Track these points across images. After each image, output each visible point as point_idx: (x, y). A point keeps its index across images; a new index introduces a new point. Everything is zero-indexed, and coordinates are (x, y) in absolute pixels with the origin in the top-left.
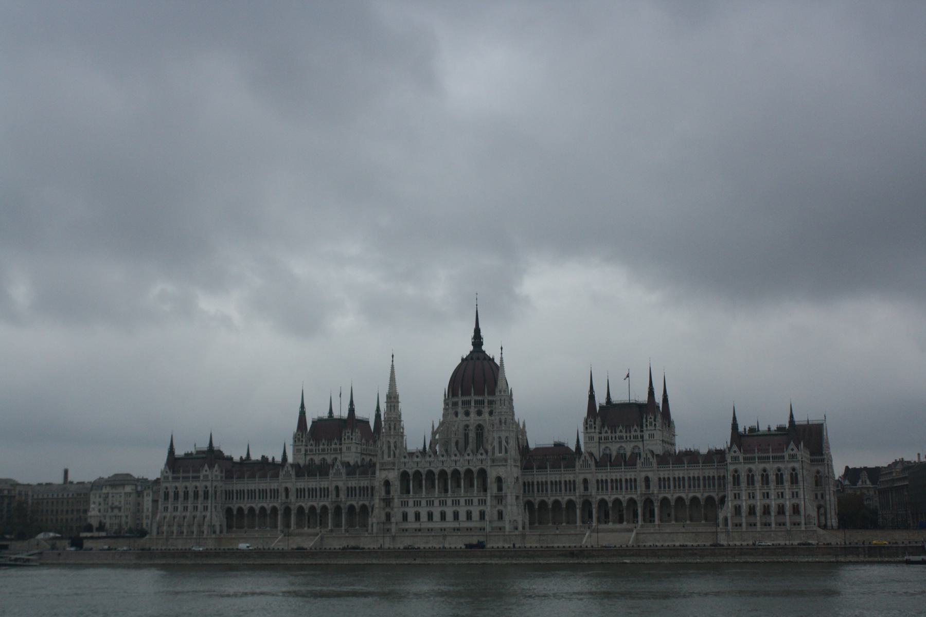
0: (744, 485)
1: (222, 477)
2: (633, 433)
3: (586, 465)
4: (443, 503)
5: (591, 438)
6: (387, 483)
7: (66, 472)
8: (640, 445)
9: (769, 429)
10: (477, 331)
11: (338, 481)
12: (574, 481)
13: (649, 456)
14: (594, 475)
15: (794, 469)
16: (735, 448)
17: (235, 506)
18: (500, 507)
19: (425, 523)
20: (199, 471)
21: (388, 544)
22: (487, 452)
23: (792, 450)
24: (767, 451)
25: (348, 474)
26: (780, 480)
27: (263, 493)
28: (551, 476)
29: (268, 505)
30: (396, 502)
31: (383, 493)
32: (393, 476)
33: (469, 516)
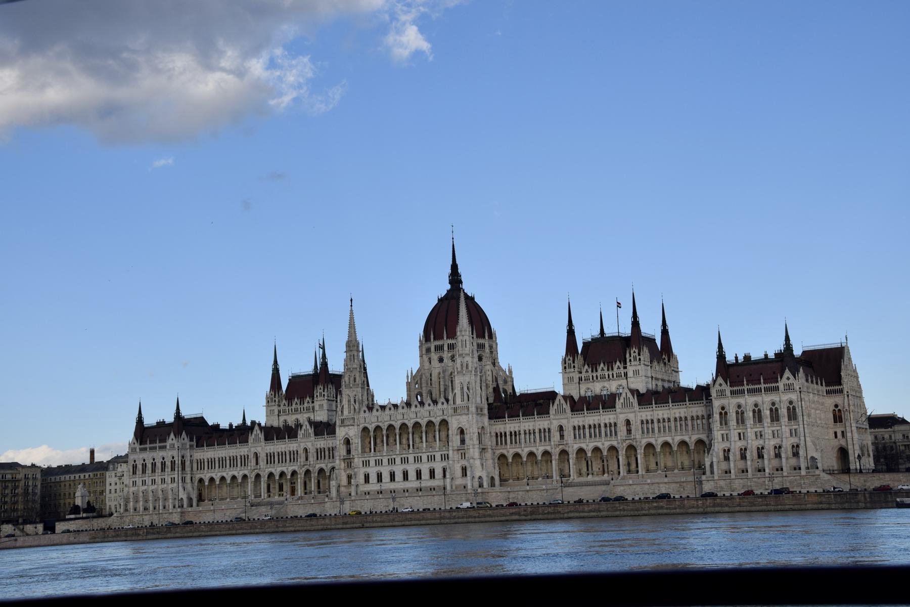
0: (733, 422)
1: (191, 446)
3: (561, 411)
4: (405, 461)
5: (571, 379)
6: (348, 442)
7: (92, 452)
9: (766, 355)
10: (454, 267)
11: (307, 441)
12: (549, 429)
13: (629, 395)
14: (571, 421)
15: (791, 402)
16: (720, 380)
17: (206, 475)
19: (387, 484)
20: (164, 440)
21: (330, 508)
22: (447, 400)
23: (788, 379)
25: (316, 435)
26: (775, 416)
27: (233, 461)
28: (523, 424)
29: (239, 473)
30: (358, 462)
32: (353, 432)
33: (432, 474)
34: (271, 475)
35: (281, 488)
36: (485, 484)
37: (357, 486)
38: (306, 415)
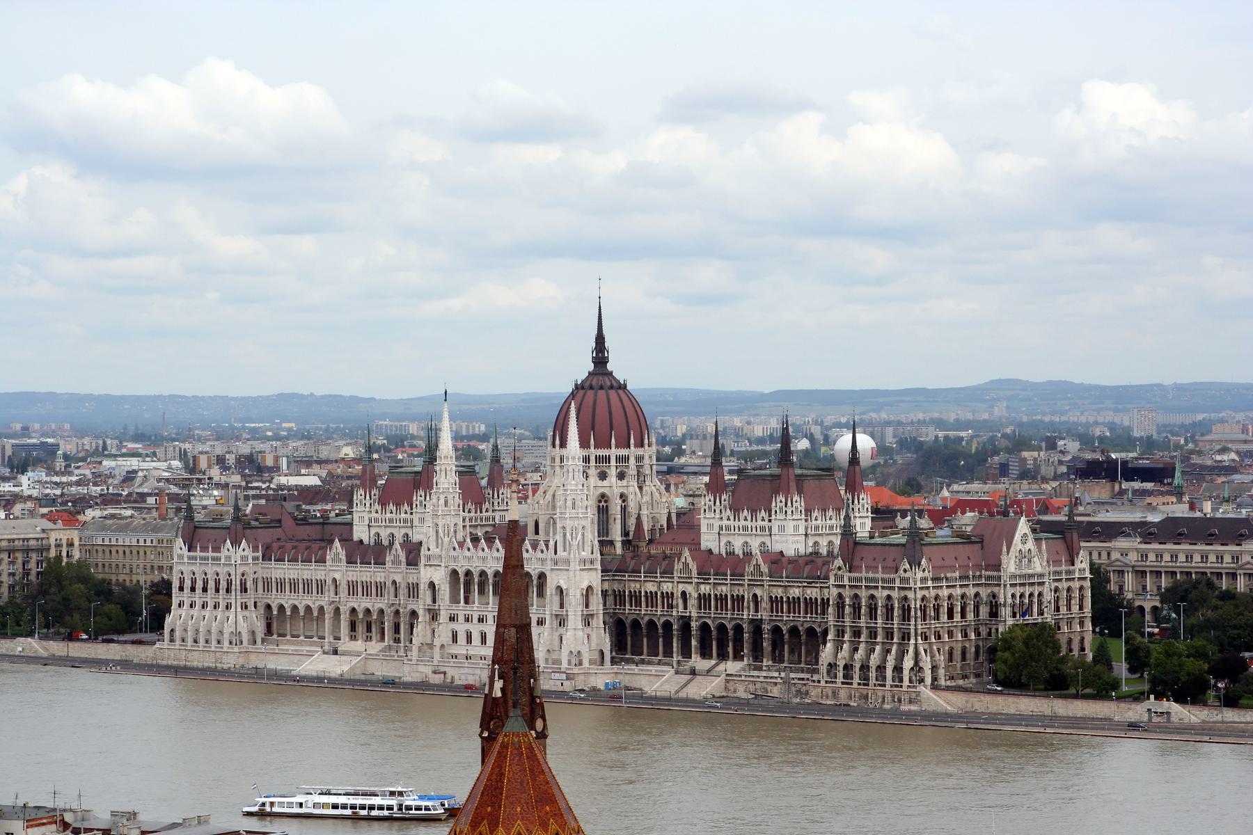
1: (255, 559)
2: (760, 523)
5: (710, 526)
6: (432, 585)
8: (767, 540)
10: (600, 339)
13: (761, 561)
17: (275, 600)
18: (562, 630)
20: (217, 549)
23: (905, 571)
24: (875, 569)
25: (408, 564)
29: (313, 601)
31: (429, 601)
32: (440, 576)
34: (353, 610)
35: (369, 629)
36: (586, 664)
37: (442, 646)
38: (403, 531)
